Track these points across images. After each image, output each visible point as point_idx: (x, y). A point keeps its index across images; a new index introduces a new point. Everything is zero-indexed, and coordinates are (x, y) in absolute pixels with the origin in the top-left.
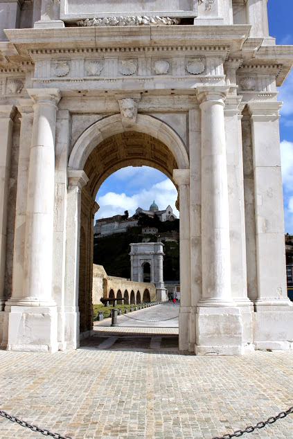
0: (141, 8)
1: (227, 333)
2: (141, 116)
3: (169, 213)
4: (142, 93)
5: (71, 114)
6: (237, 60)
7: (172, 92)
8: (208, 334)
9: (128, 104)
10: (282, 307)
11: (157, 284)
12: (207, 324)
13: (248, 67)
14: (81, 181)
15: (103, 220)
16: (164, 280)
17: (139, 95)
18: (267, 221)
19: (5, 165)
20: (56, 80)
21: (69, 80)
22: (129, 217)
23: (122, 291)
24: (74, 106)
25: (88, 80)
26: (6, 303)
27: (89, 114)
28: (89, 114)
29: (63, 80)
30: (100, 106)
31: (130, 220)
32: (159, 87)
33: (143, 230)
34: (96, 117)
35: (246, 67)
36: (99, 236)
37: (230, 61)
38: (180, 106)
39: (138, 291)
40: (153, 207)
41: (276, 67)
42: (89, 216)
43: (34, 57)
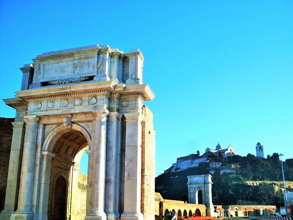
0: (73, 73)
2: (74, 125)
5: (45, 125)
9: (65, 120)
11: (207, 206)
13: (124, 95)
15: (181, 158)
16: (213, 202)
18: (129, 174)
22: (200, 155)
24: (45, 121)
25: (48, 110)
27: (52, 124)
28: (52, 124)
29: (39, 111)
30: (55, 120)
31: (202, 157)
32: (77, 112)
33: (210, 165)
34: (55, 126)
35: (123, 96)
38: (89, 119)
41: (137, 94)
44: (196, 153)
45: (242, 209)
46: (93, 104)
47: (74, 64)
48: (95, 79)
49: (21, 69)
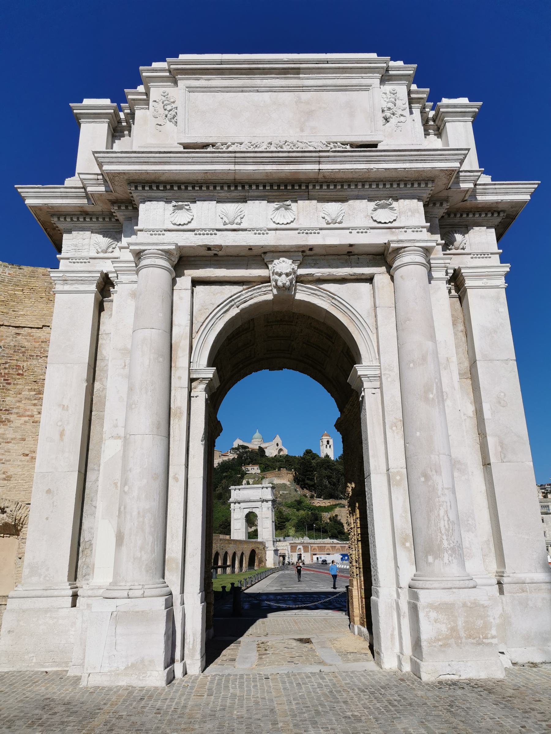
1: (470, 636)
4: (303, 252)
6: (441, 204)
7: (350, 249)
8: (439, 640)
12: (436, 621)
17: (300, 254)
21: (193, 230)
23: (221, 554)
45: (310, 550)
46: (385, 223)
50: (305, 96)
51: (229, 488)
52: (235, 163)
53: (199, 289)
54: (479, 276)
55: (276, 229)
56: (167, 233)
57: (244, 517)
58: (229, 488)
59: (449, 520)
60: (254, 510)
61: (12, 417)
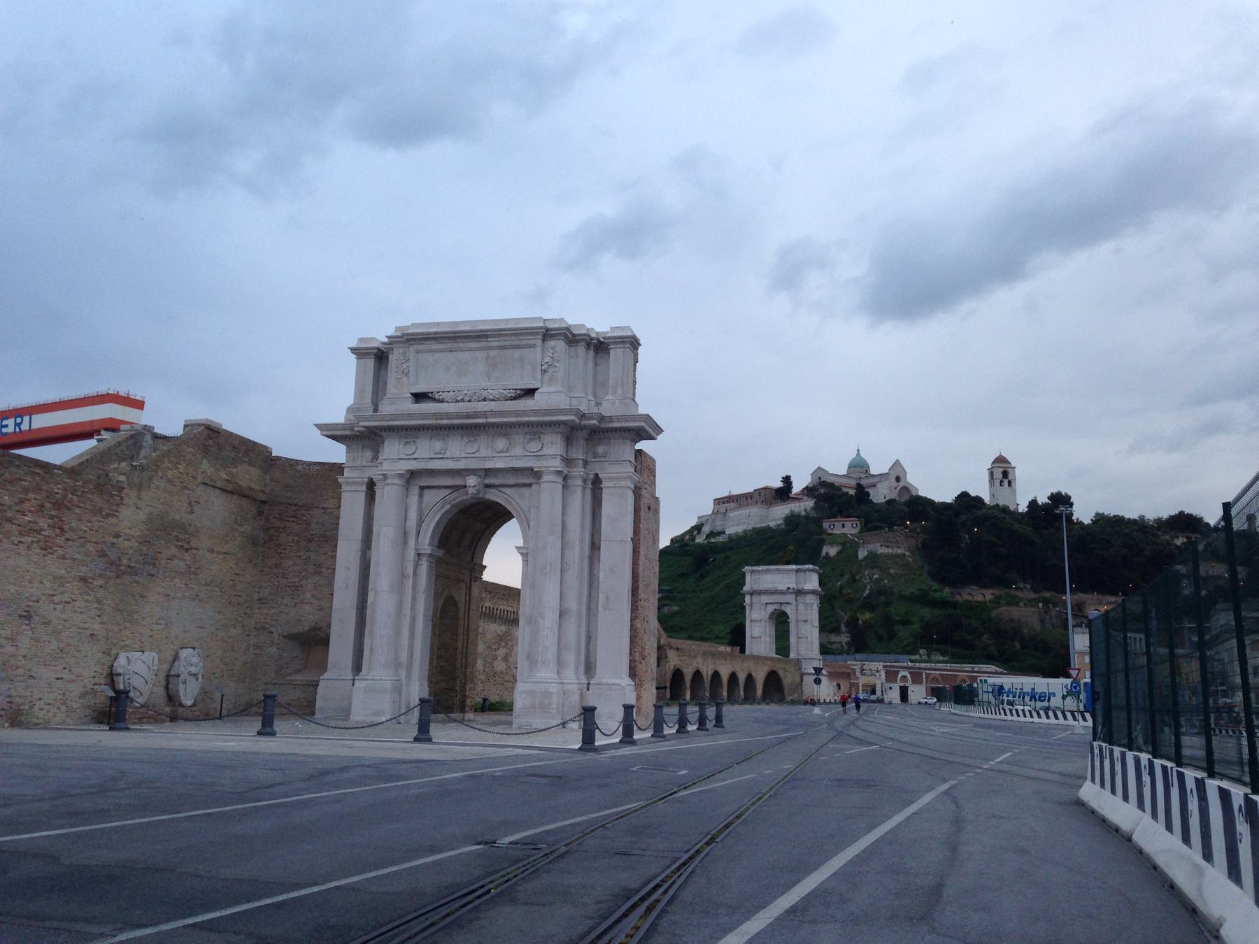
0: (487, 379)
3: (898, 479)
8: (524, 709)
10: (614, 687)
12: (525, 699)
14: (430, 555)
18: (607, 598)
19: (360, 538)
20: (403, 459)
21: (416, 459)
23: (704, 674)
26: (356, 678)
36: (721, 539)
37: (575, 431)
39: (750, 678)
40: (859, 465)
42: (468, 581)
43: (383, 433)
44: (778, 484)
45: (924, 680)
47: (487, 358)
48: (537, 394)
49: (353, 350)
50: (492, 353)
51: (743, 570)
52: (436, 419)
53: (426, 491)
54: (611, 479)
55: (466, 458)
56: (401, 462)
57: (767, 617)
58: (743, 570)
59: (544, 645)
60: (783, 608)
61: (324, 570)
